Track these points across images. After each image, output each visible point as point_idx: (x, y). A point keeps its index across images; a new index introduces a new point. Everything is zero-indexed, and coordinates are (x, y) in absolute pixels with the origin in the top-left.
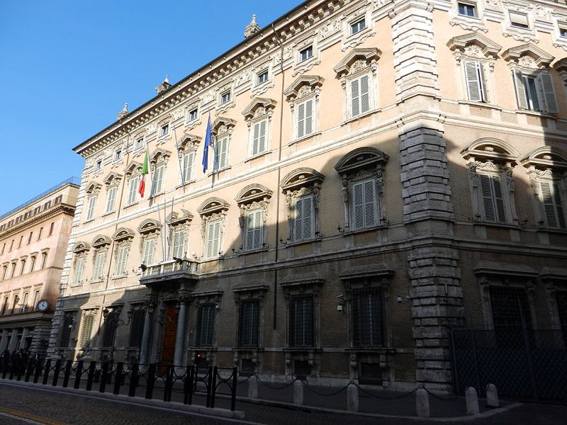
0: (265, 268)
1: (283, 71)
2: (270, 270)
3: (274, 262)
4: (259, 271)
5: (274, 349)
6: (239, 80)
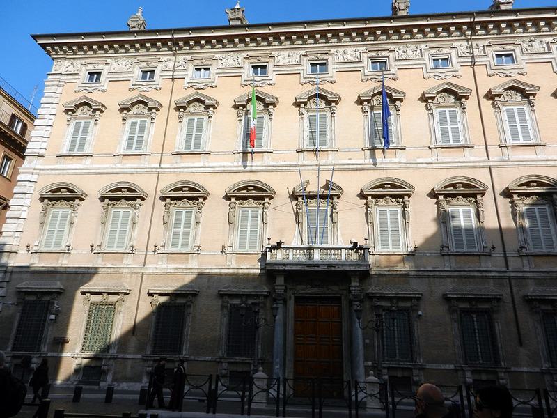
0: (493, 274)
1: (474, 65)
2: (501, 278)
4: (482, 277)
5: (525, 369)
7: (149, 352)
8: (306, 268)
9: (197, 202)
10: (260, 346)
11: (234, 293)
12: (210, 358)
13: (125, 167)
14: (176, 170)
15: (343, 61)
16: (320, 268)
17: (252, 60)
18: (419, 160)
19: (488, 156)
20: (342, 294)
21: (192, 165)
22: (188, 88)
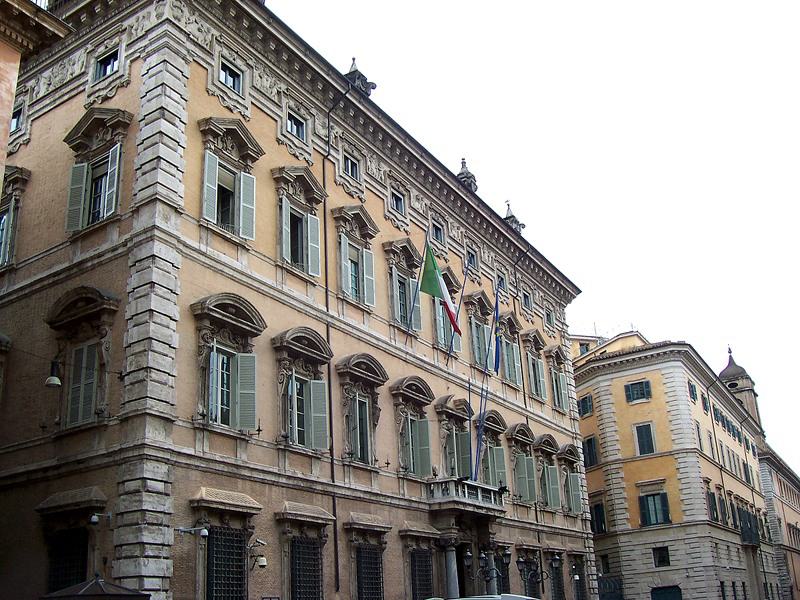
2: (535, 530)
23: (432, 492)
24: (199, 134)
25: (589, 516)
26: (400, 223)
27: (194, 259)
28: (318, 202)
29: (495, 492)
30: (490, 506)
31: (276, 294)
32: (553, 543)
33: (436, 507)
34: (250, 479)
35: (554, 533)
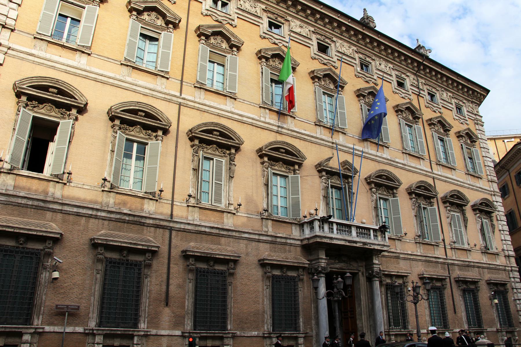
2: (444, 263)
3: (445, 257)
6: (378, 63)
7: (189, 328)
8: (348, 244)
9: (228, 152)
10: (301, 320)
11: (279, 263)
12: (256, 333)
13: (136, 82)
14: (200, 106)
15: (340, 50)
16: (358, 245)
17: (269, 15)
18: (397, 160)
19: (432, 169)
20: (360, 271)
21: (218, 106)
22: (206, 15)
23: (303, 231)
24: (310, 80)
25: (512, 253)
26: (435, 109)
27: (23, 59)
28: (419, 118)
29: (375, 230)
30: (368, 241)
31: (116, 82)
32: (466, 273)
33: (305, 242)
34: (61, 211)
35: (468, 266)
